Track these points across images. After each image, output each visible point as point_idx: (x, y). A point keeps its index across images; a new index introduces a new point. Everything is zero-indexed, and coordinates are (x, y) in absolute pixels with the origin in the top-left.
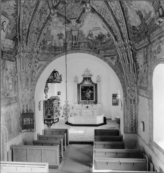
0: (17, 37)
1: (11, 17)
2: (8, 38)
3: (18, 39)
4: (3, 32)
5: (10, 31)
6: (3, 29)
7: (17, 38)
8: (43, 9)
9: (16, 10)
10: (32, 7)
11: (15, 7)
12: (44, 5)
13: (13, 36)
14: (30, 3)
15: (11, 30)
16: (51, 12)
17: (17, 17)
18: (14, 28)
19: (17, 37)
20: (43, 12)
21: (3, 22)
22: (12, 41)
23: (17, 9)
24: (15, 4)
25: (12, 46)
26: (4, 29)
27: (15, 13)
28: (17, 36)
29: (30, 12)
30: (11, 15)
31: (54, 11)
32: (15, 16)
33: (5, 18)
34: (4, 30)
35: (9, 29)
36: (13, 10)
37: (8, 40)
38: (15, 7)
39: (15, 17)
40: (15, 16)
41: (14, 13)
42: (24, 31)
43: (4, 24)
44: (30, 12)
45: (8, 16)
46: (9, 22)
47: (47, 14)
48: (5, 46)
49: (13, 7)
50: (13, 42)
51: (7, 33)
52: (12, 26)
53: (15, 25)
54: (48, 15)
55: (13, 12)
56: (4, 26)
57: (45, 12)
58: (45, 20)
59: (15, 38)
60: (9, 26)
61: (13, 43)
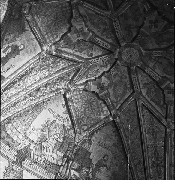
30: (113, 145)
31: (166, 120)
34: (107, 167)
41: (116, 143)
46: (112, 155)
57: (158, 129)
58: (163, 141)
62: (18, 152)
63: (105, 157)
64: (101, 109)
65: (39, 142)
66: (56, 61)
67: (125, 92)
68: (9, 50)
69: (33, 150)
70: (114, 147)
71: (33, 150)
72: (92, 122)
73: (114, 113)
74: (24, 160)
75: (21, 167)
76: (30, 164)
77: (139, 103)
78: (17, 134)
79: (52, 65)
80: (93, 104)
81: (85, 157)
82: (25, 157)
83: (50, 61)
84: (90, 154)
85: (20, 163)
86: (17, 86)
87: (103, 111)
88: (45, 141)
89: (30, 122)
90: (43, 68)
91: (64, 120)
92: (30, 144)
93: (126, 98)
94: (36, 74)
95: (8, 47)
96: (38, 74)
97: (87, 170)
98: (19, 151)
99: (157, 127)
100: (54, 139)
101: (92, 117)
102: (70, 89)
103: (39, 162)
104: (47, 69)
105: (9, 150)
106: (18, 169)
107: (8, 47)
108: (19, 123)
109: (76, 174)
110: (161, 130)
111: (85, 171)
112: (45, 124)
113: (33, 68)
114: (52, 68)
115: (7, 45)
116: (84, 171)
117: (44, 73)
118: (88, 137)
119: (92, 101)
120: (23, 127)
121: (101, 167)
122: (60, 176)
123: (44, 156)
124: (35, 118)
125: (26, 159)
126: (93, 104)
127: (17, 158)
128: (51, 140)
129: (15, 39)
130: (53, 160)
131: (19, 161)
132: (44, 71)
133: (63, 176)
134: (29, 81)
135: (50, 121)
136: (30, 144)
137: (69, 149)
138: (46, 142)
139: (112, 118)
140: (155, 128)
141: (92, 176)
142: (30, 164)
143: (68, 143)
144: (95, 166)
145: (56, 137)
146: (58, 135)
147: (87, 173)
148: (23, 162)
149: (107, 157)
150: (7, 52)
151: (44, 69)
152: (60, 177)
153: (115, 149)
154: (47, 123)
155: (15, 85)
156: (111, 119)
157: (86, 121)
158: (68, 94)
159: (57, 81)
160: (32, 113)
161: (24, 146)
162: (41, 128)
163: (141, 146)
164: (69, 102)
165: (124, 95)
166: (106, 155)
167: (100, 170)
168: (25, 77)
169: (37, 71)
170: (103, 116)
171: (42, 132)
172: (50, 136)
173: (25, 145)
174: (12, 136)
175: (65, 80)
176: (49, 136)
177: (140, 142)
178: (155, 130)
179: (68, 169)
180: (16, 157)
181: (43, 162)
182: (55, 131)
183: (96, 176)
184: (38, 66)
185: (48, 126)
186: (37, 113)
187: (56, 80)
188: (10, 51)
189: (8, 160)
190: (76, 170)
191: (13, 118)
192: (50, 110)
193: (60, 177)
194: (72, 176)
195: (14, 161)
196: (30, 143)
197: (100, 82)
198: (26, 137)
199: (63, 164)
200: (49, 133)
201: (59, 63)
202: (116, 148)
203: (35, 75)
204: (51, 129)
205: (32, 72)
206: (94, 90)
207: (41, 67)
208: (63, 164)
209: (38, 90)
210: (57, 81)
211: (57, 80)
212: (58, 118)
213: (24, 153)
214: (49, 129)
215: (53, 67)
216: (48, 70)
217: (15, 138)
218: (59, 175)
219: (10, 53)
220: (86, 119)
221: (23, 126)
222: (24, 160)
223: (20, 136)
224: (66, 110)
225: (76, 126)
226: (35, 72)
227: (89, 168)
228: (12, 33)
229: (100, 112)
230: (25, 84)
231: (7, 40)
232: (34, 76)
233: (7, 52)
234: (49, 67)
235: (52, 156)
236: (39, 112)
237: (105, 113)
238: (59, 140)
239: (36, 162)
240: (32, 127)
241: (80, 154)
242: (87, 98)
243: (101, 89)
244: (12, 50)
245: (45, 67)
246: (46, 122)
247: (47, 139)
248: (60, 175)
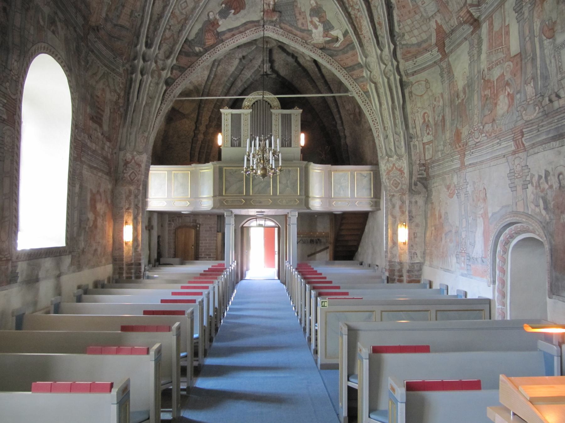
68: (316, 20)
86: (359, 13)
95: (311, 22)
107: (311, 22)
108: (409, 22)
115: (309, 24)
129: (303, 12)
150: (318, 23)
155: (358, 16)
188: (317, 19)
191: (400, 29)
196: (434, 20)
219: (319, 18)
223: (424, 28)
228: (296, 17)
231: (303, 24)
233: (318, 23)
244: (316, 16)
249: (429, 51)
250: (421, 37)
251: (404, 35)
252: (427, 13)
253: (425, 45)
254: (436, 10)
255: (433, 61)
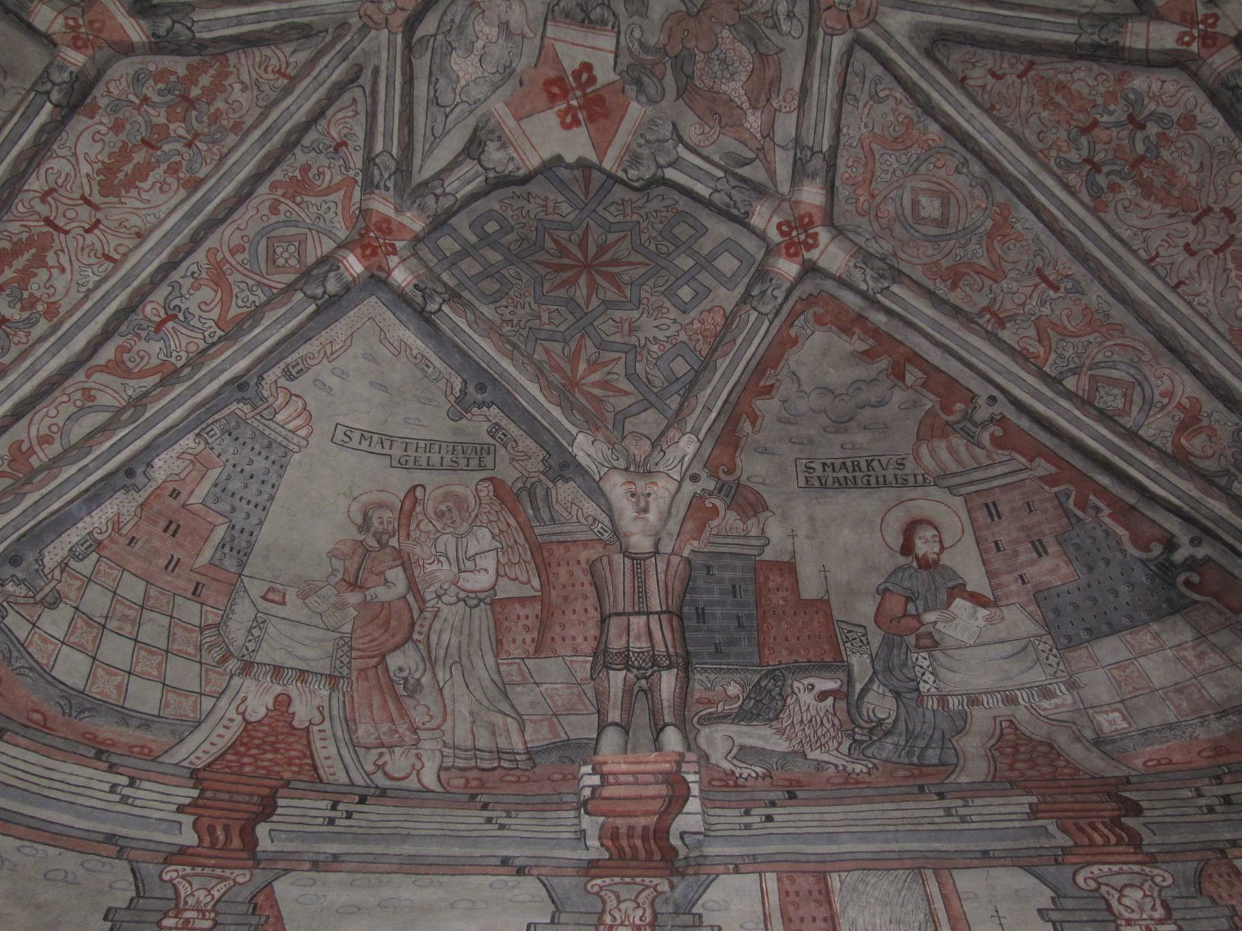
0: (1179, 556)
1: (932, 452)
2: (1095, 635)
3: (1208, 559)
4: (983, 612)
5: (1046, 563)
6: (958, 590)
7: (1191, 564)
8: (1096, 131)
9: (913, 375)
10: (1002, 228)
11: (883, 363)
12: (1050, 104)
13: (1140, 576)
14: (943, 222)
15: (1050, 542)
16: (1175, 61)
17: (983, 413)
18: (1067, 513)
19: (1179, 556)
20: (1140, 148)
21: (897, 542)
22: (1179, 633)
23: (916, 359)
24: (862, 347)
25: (1210, 671)
26: (976, 580)
27: (929, 401)
28: (1170, 544)
29: (1039, 272)
30: (920, 439)
32: (967, 416)
33: (890, 494)
34: (977, 599)
35: (1026, 554)
36: (899, 396)
37: (1110, 649)
38: (883, 363)
39: (968, 429)
40: (967, 416)
42: (1196, 444)
43: (923, 547)
44: (1039, 272)
45: (901, 465)
46: (958, 502)
47: (1189, 122)
48: (1111, 722)
49: (871, 382)
50: (1188, 635)
51: (1040, 596)
52: (1030, 508)
53: (1050, 480)
54: (1208, 113)
55: (915, 404)
56: (946, 559)
57: (1153, 129)
59: (1173, 585)
60: (1005, 532)
61: (1201, 637)
62: (196, 776)
63: (918, 543)
64: (685, 263)
65: (357, 664)
66: (195, 92)
67: (762, 57)
69: (327, 725)
70: (941, 446)
71: (327, 725)
72: (680, 367)
73: (776, 220)
74: (272, 814)
75: (251, 863)
76: (331, 821)
77: (888, 36)
78: (148, 664)
79: (178, 128)
80: (614, 262)
81: (758, 604)
82: (266, 792)
83: (154, 105)
84: (789, 568)
85: (236, 842)
87: (706, 263)
88: (409, 638)
89: (231, 564)
90: (128, 168)
91: (482, 450)
92: (283, 703)
93: (797, 85)
94: (98, 222)
96: (113, 215)
97: (831, 685)
98: (202, 775)
99: (1131, 119)
100: (471, 600)
101: (661, 336)
102: (388, 220)
103: (412, 783)
104: (164, 166)
105: (113, 788)
106: (222, 887)
108: (133, 589)
109: (749, 742)
110: (1175, 114)
111: (823, 696)
112: (362, 537)
113: (51, 192)
114: (189, 145)
116: (807, 698)
117: (156, 197)
118: (713, 475)
119: (603, 249)
120: (190, 611)
121: (930, 617)
122: (604, 782)
123: (437, 734)
124: (261, 523)
125: (281, 802)
126: (614, 262)
127: (200, 817)
128: (451, 613)
130: (523, 732)
131: (221, 835)
132: (145, 185)
133: (634, 774)
134: (61, 282)
135: (381, 506)
136: (283, 703)
137: (608, 609)
138: (416, 642)
139: (790, 256)
140: (1132, 138)
141: (890, 702)
142: (331, 821)
143: (587, 579)
144: (876, 638)
145: (481, 581)
146: (489, 562)
147: (842, 704)
148: (262, 830)
149: (929, 533)
151: (142, 172)
152: (607, 792)
153: (951, 450)
154: (365, 526)
156: (788, 268)
157: (631, 376)
158: (393, 260)
159: (274, 219)
160: (217, 500)
161: (237, 727)
162: (334, 570)
163: (1118, 313)
164: (433, 307)
165: (776, 82)
166: (910, 530)
167: (930, 635)
168: (20, 263)
169: (97, 198)
170: (722, 291)
171: (354, 598)
172: (429, 595)
173: (243, 714)
174: (113, 697)
175: (329, 190)
176: (422, 600)
177: (1096, 295)
178: (1140, 148)
179: (666, 725)
180: (187, 820)
181: (441, 768)
182: (452, 555)
183: (923, 687)
184: (85, 168)
185: (383, 545)
186: (254, 486)
187: (265, 210)
189: (119, 857)
190: (744, 716)
191: (64, 566)
192: (345, 437)
193: (607, 792)
194: (726, 765)
195: (183, 850)
196: (278, 689)
197: (552, 74)
198: (233, 665)
199: (615, 715)
200: (412, 585)
201: (221, 97)
202: (958, 442)
203: (87, 231)
204: (420, 551)
205: (60, 222)
206: (557, 151)
207: (108, 171)
208: (615, 715)
209: (164, 322)
210: (274, 219)
211: (274, 210)
212: (435, 459)
213: (248, 769)
214: (405, 562)
215: (196, 135)
216: (174, 169)
217: (145, 697)
218: (596, 780)
220: (619, 368)
221: (179, 600)
222: (267, 809)
223: (183, 673)
224: (457, 383)
225: (574, 430)
226: (84, 212)
227: (835, 663)
229: (689, 277)
230: (40, 308)
232: (90, 238)
234: (166, 148)
235: (507, 709)
236: (273, 478)
237: (727, 264)
238: (507, 589)
239: (383, 793)
240: (256, 589)
241: (711, 604)
242: (549, 244)
243: (591, 119)
245: (140, 156)
246: (359, 521)
247: (413, 624)
248: (603, 776)
249: (112, 768)
250: (123, 690)
251: (54, 602)
252: (258, 641)
253: (107, 729)
254: (324, 666)
255: (106, 828)
